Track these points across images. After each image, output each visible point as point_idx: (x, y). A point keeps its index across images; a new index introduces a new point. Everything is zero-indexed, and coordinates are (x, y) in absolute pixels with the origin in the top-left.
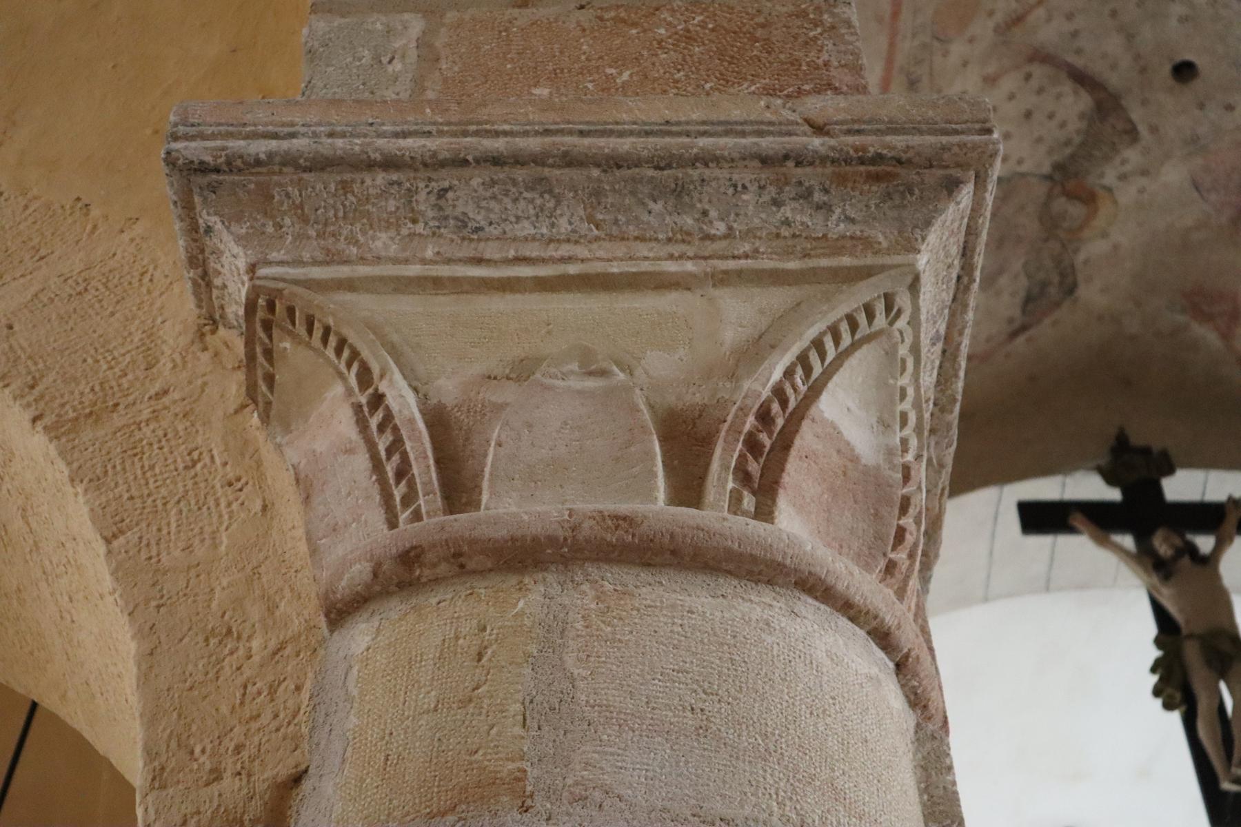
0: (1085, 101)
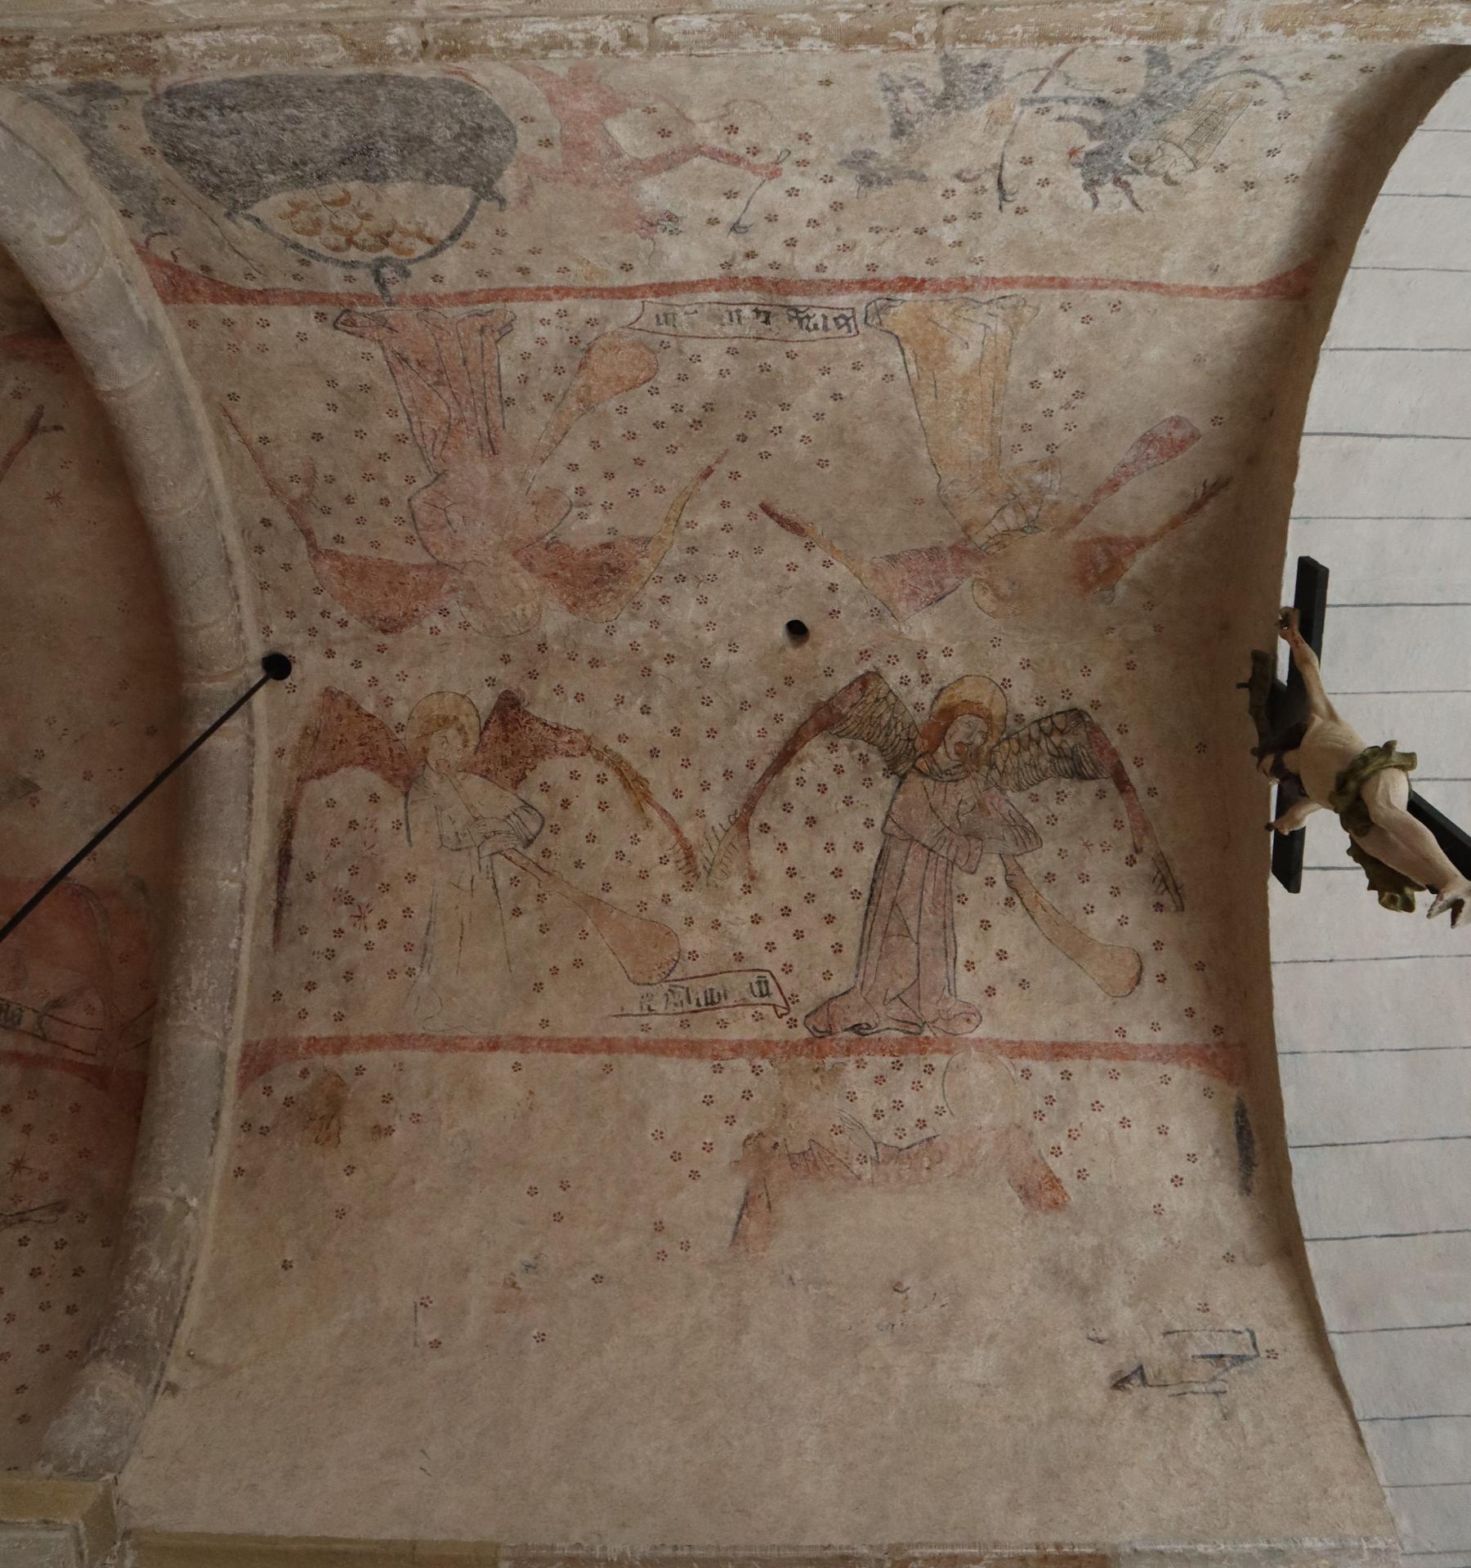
0: (815, 748)
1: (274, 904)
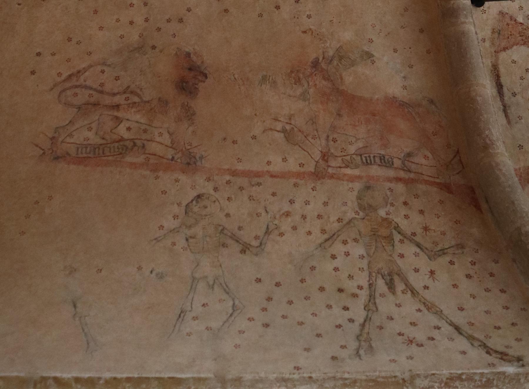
1: (502, 107)
